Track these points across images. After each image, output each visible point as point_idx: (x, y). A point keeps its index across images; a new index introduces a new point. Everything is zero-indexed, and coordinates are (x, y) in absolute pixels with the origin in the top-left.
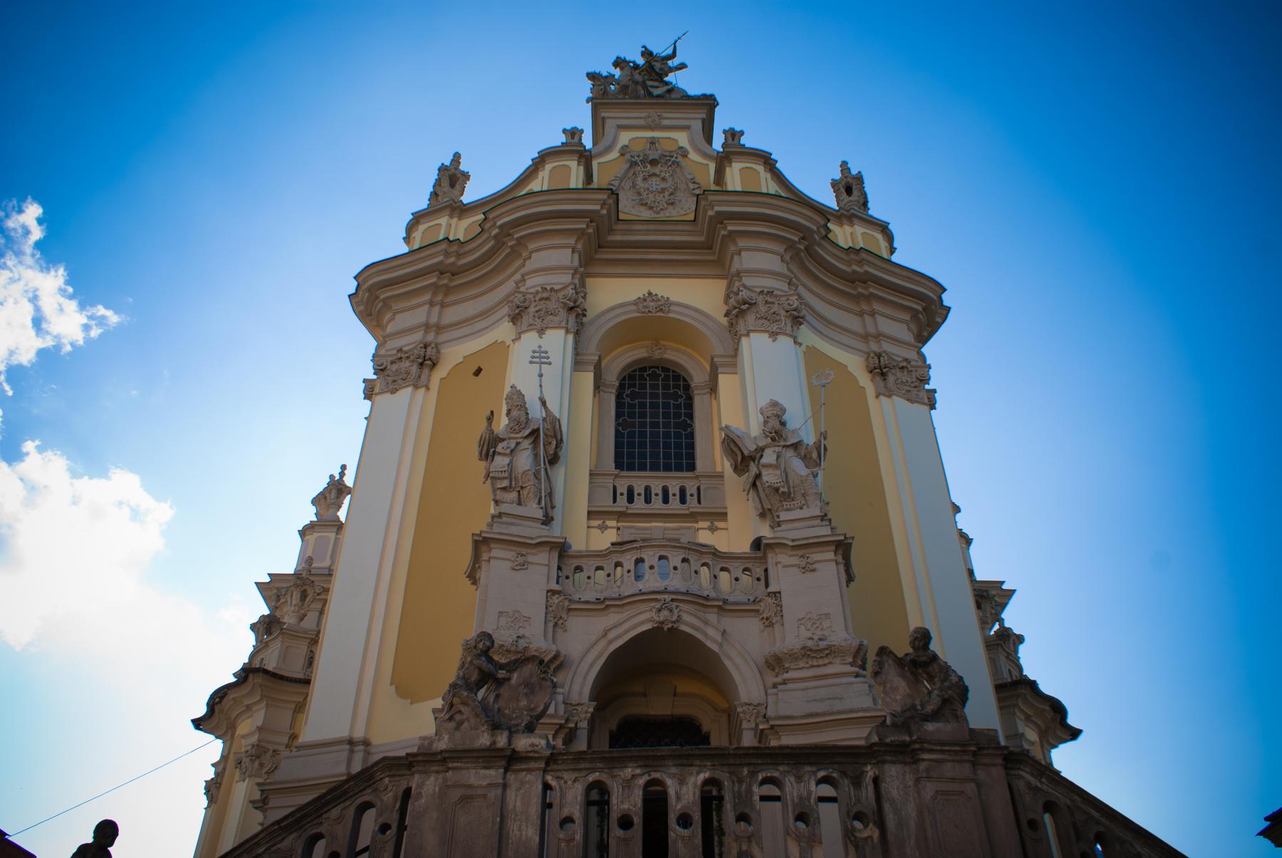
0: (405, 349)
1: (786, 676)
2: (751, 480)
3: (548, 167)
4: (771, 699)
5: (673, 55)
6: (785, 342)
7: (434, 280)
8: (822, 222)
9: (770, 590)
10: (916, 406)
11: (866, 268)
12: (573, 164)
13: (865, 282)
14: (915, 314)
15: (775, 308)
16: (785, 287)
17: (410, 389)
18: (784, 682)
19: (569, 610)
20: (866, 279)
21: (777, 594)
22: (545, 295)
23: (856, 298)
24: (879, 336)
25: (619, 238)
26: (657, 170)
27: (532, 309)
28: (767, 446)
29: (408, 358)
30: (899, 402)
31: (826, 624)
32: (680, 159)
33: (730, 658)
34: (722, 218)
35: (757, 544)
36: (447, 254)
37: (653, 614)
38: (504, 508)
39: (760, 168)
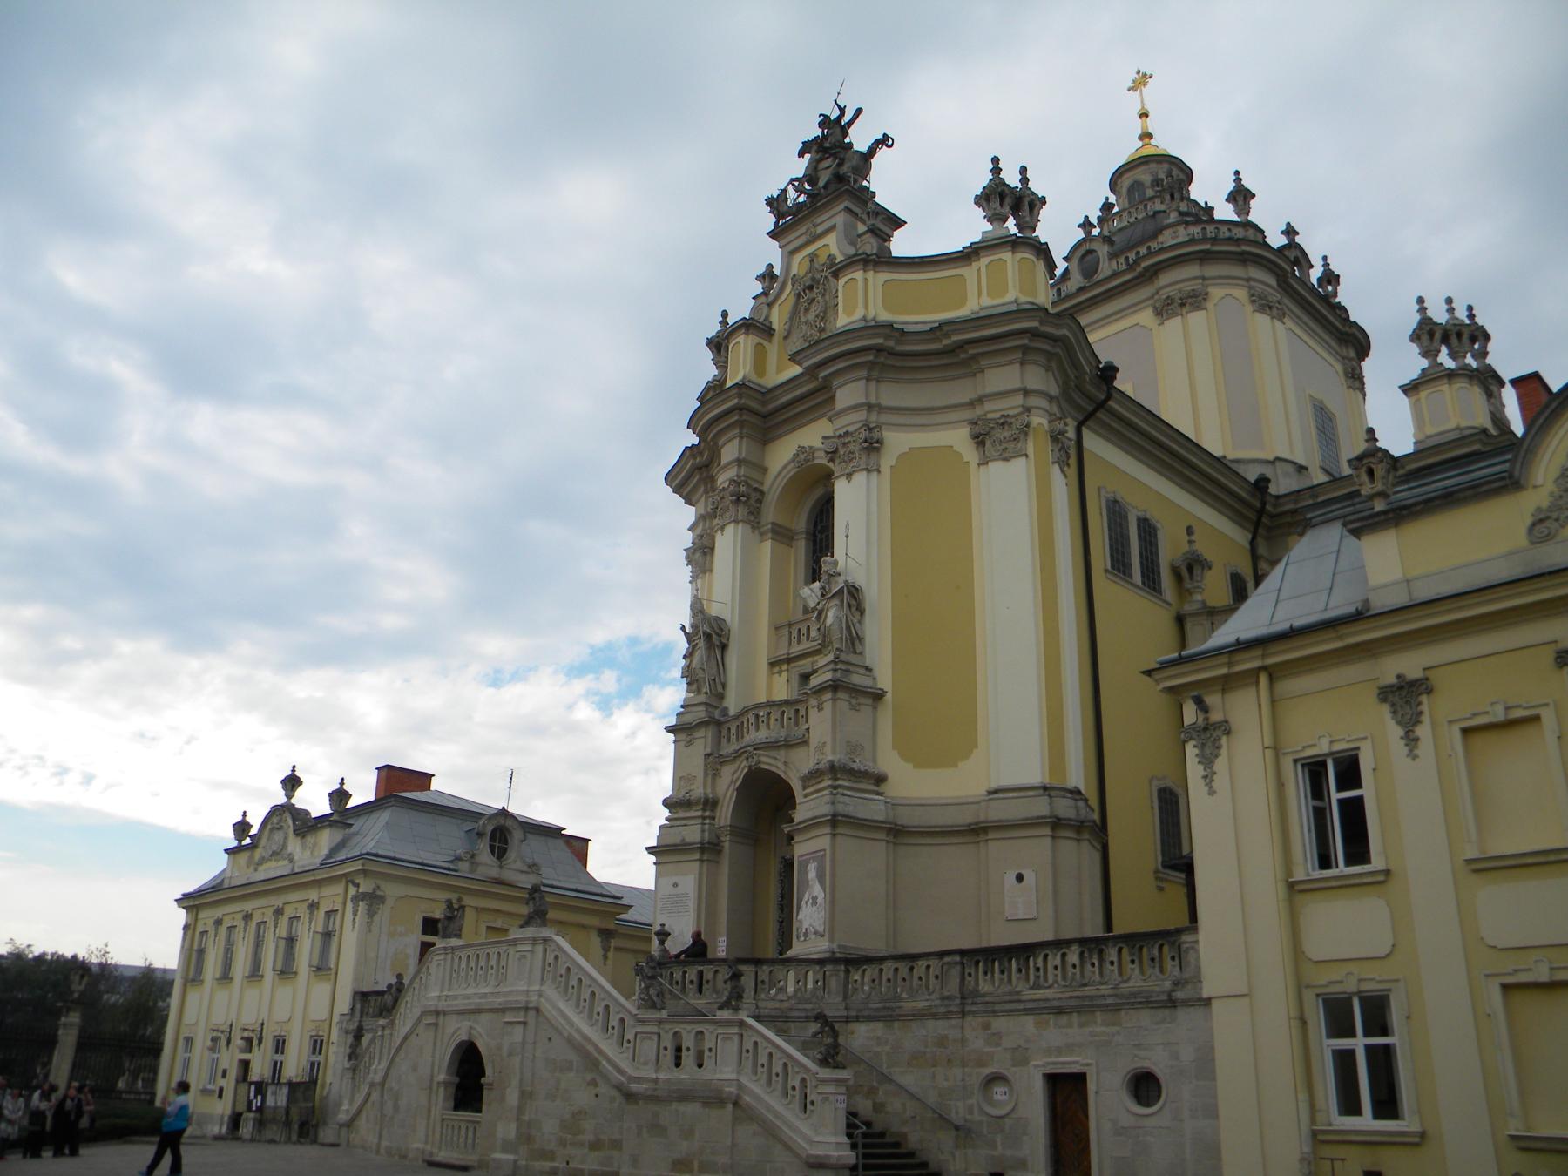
5: (842, 110)
6: (860, 478)
8: (887, 331)
10: (1014, 461)
11: (955, 338)
13: (961, 347)
14: (1026, 350)
15: (852, 447)
16: (861, 416)
19: (721, 764)
20: (961, 346)
23: (964, 363)
24: (980, 400)
25: (771, 406)
30: (996, 467)
36: (693, 456)
39: (859, 275)
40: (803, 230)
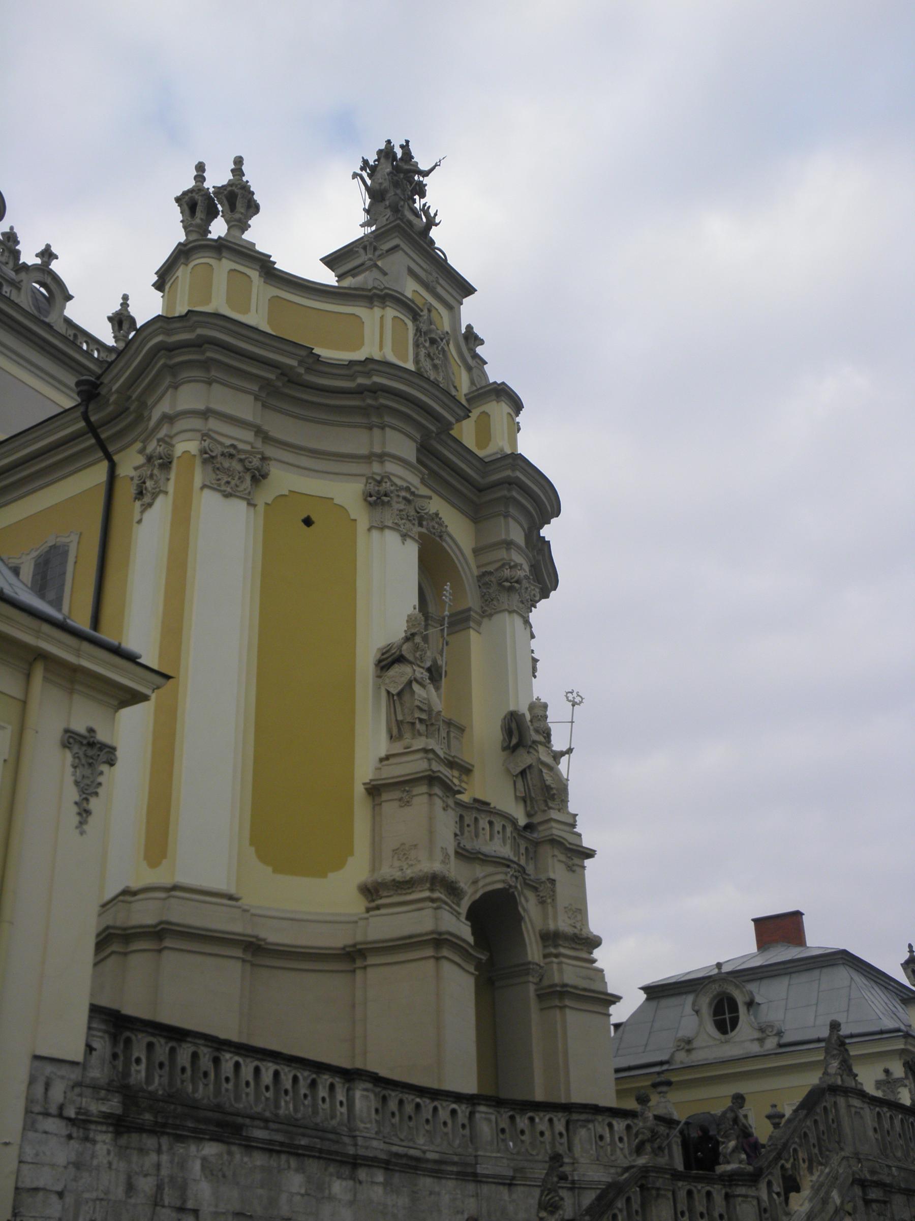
0: (241, 446)
1: (563, 950)
2: (524, 766)
3: (391, 313)
4: (555, 966)
7: (272, 376)
9: (552, 876)
12: (410, 324)
17: (244, 504)
18: (557, 956)
21: (553, 881)
22: (408, 496)
26: (433, 350)
27: (396, 506)
28: (540, 743)
29: (241, 460)
31: (579, 917)
32: (446, 349)
33: (525, 922)
34: (511, 483)
35: (529, 827)
36: (301, 363)
37: (508, 878)
38: (432, 744)
40: (425, 266)
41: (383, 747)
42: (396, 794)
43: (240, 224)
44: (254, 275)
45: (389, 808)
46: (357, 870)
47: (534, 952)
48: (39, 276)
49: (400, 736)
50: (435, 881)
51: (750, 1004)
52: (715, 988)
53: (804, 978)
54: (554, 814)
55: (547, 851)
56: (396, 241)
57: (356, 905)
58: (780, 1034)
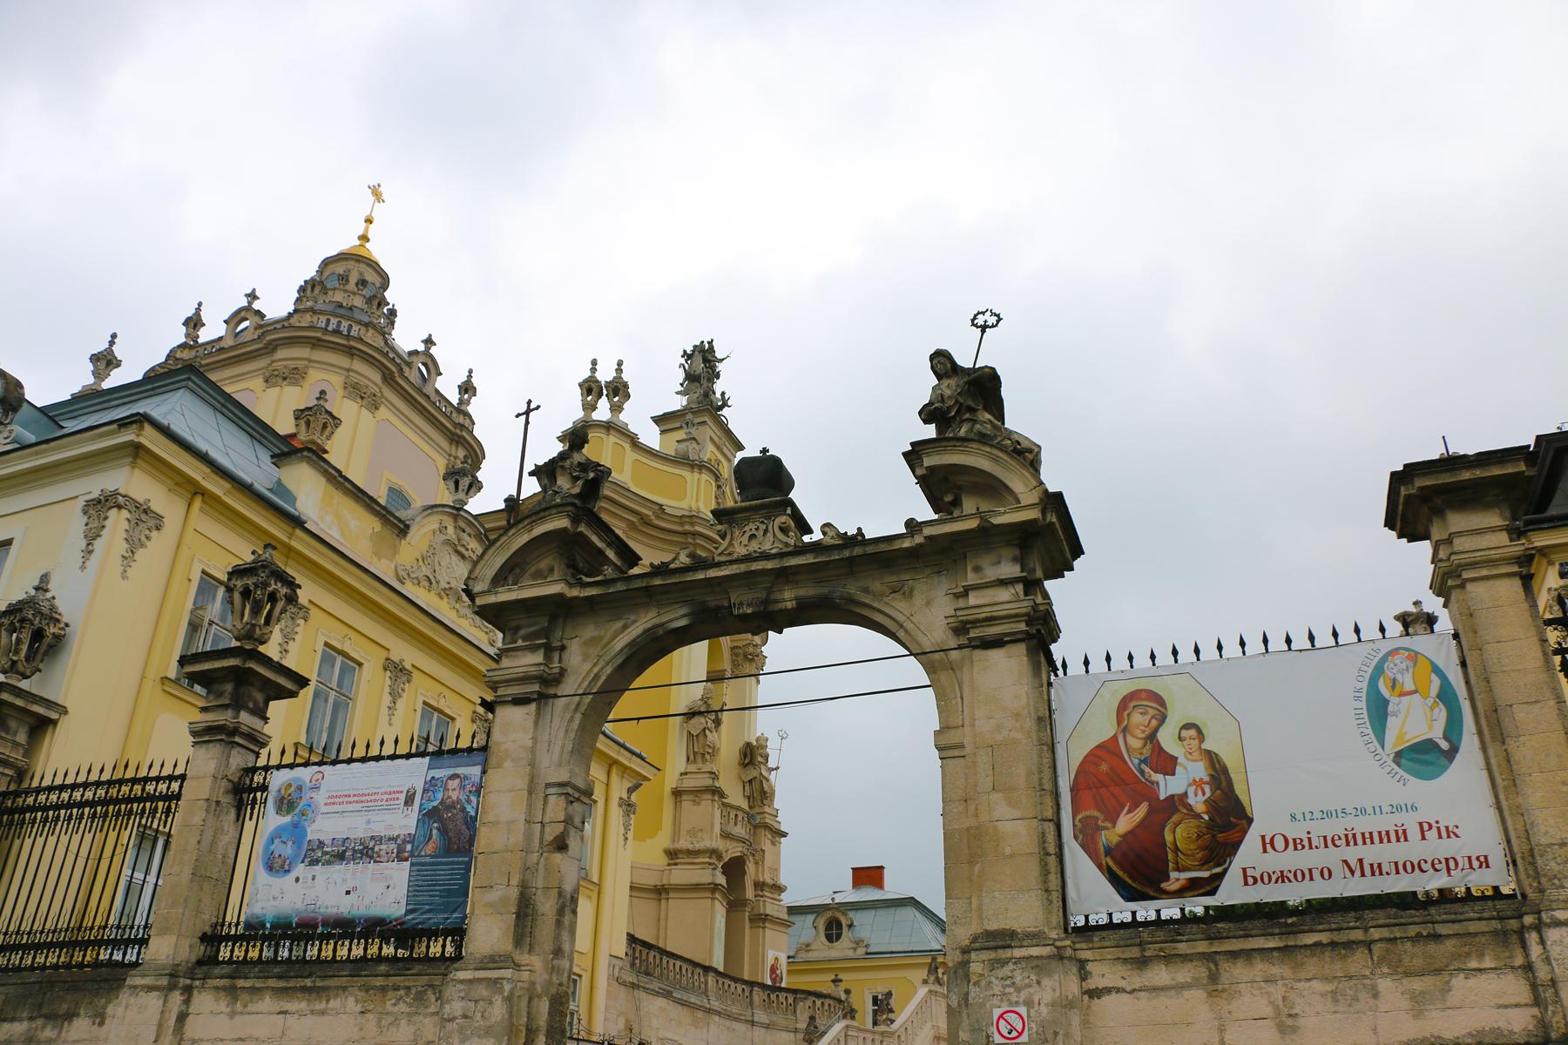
41: (681, 765)
42: (691, 797)
43: (616, 409)
44: (627, 446)
45: (687, 804)
46: (663, 840)
47: (750, 893)
48: (423, 358)
49: (695, 761)
50: (714, 852)
51: (850, 926)
52: (829, 914)
53: (881, 912)
54: (767, 809)
55: (762, 831)
56: (706, 419)
57: (663, 860)
58: (867, 946)
